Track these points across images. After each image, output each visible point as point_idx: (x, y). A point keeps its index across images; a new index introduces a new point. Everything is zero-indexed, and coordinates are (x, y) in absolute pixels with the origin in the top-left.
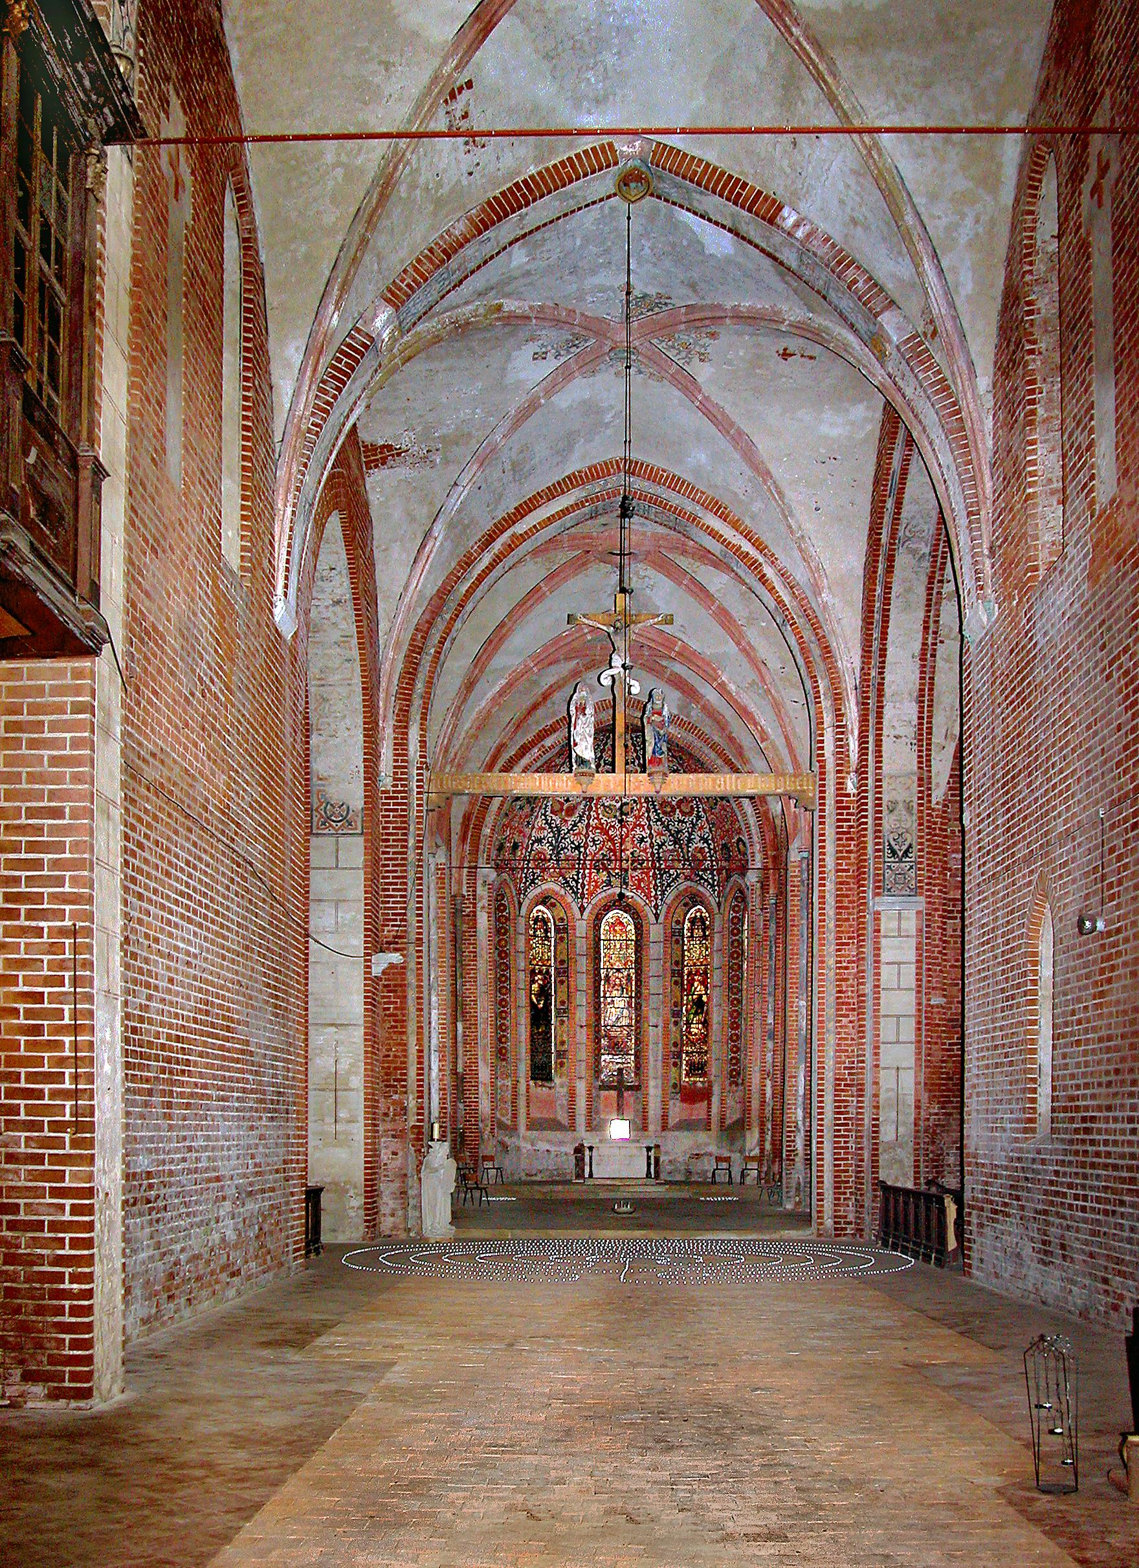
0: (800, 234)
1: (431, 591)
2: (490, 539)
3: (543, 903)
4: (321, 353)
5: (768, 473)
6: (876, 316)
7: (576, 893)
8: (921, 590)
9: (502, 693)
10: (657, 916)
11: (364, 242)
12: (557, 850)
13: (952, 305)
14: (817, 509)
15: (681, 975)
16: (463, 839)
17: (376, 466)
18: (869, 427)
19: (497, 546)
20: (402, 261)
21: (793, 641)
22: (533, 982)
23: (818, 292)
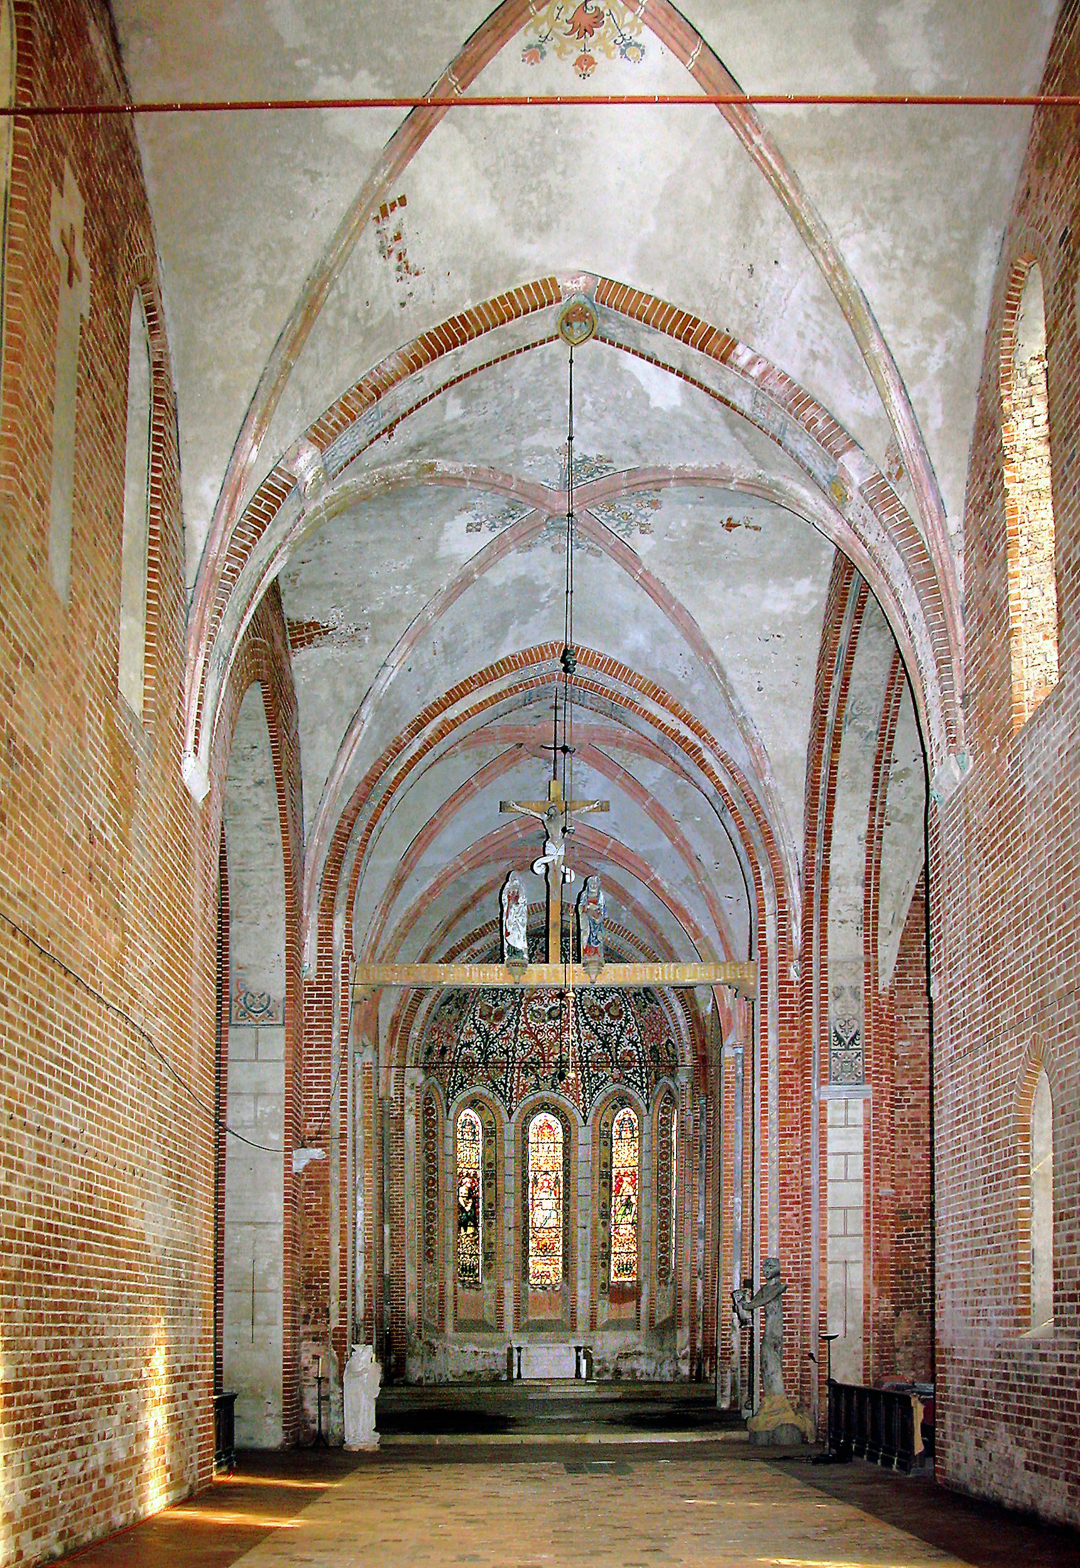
0: (755, 372)
1: (359, 777)
2: (418, 726)
4: (237, 490)
5: (710, 652)
6: (838, 456)
7: (504, 1097)
8: (868, 772)
9: (432, 891)
11: (287, 368)
13: (920, 440)
14: (759, 689)
16: (392, 1042)
17: (302, 645)
18: (815, 602)
19: (428, 731)
20: (328, 398)
21: (733, 828)
22: (461, 1185)
23: (773, 437)
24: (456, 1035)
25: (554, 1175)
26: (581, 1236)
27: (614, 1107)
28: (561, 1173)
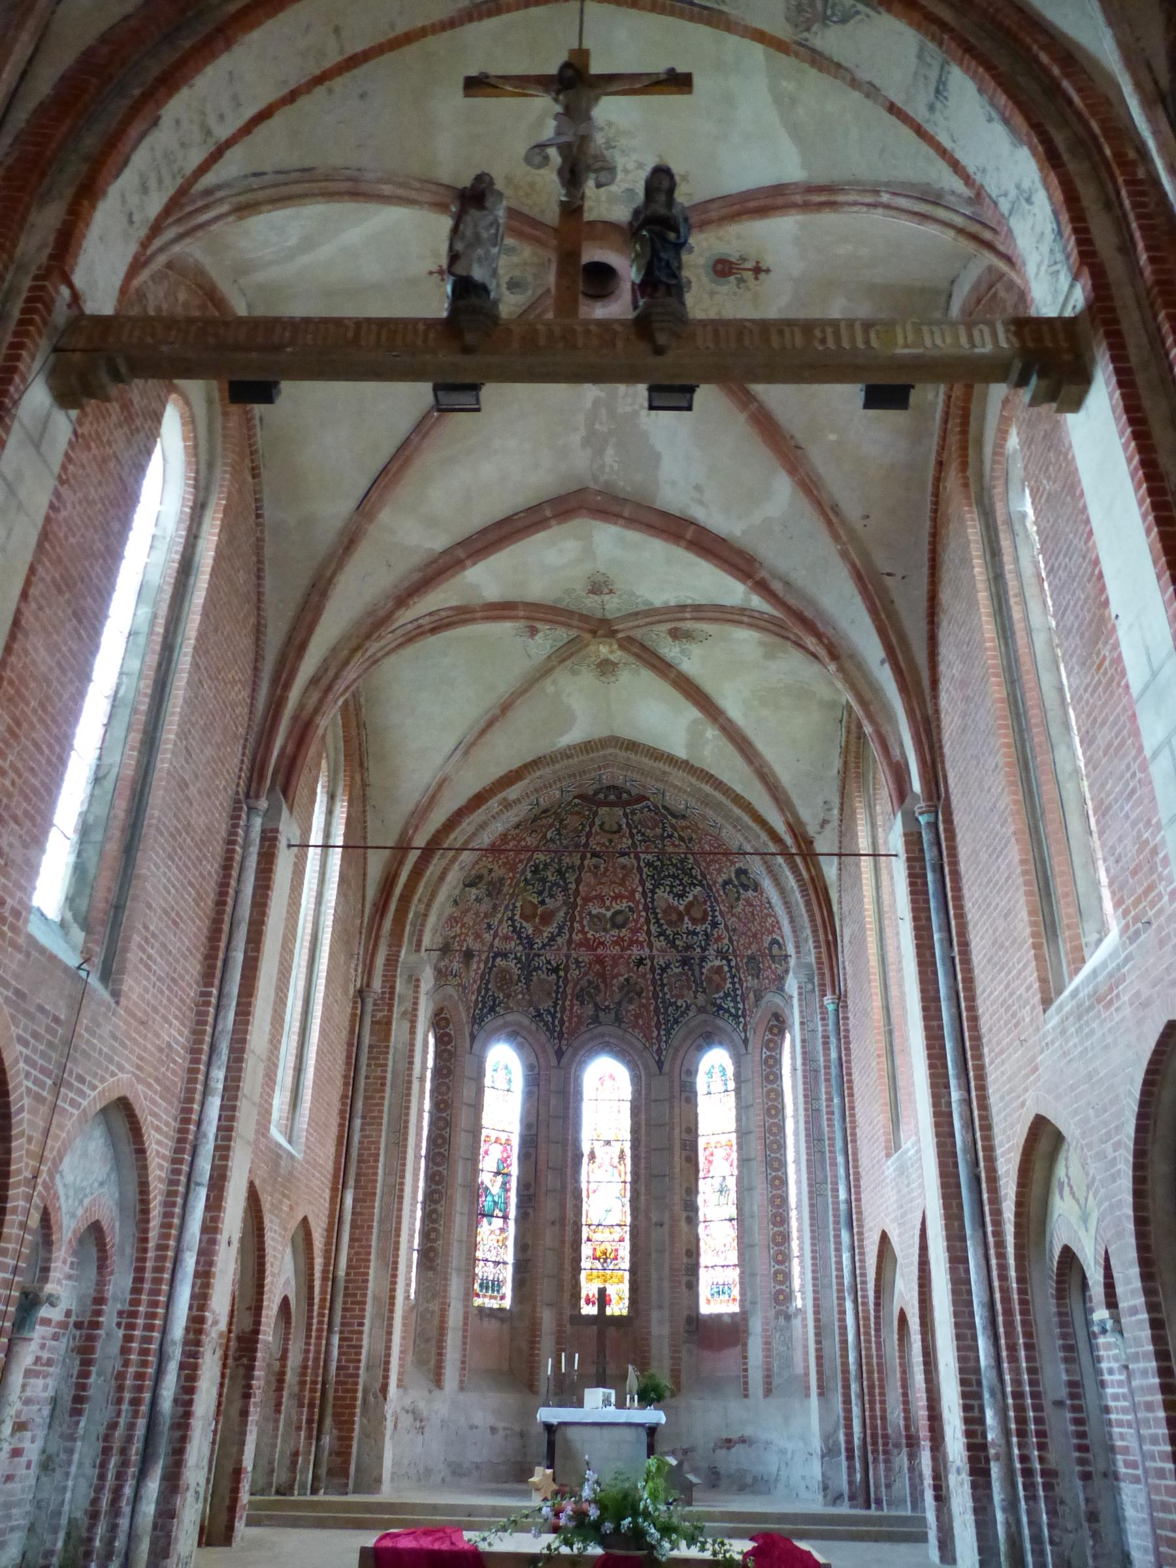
12: (528, 969)
24: (488, 937)
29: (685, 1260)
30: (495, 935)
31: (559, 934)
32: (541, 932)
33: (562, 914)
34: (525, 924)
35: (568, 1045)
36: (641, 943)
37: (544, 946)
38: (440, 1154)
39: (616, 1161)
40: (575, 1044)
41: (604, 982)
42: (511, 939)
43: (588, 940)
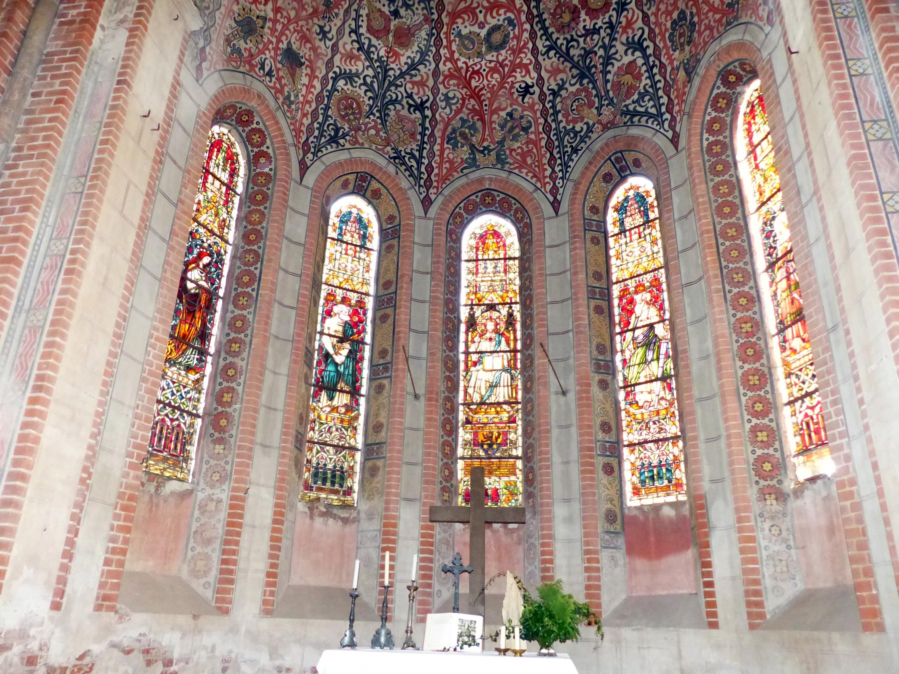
3: (359, 190)
10: (556, 205)
12: (383, 105)
15: (607, 295)
25: (504, 311)
26: (559, 409)
27: (607, 178)
28: (516, 308)
29: (601, 436)
30: (335, 48)
31: (421, 62)
32: (397, 55)
33: (423, 34)
34: (374, 41)
35: (438, 194)
36: (526, 66)
37: (402, 75)
38: (244, 294)
39: (502, 327)
40: (446, 192)
41: (482, 119)
42: (358, 58)
43: (459, 70)
